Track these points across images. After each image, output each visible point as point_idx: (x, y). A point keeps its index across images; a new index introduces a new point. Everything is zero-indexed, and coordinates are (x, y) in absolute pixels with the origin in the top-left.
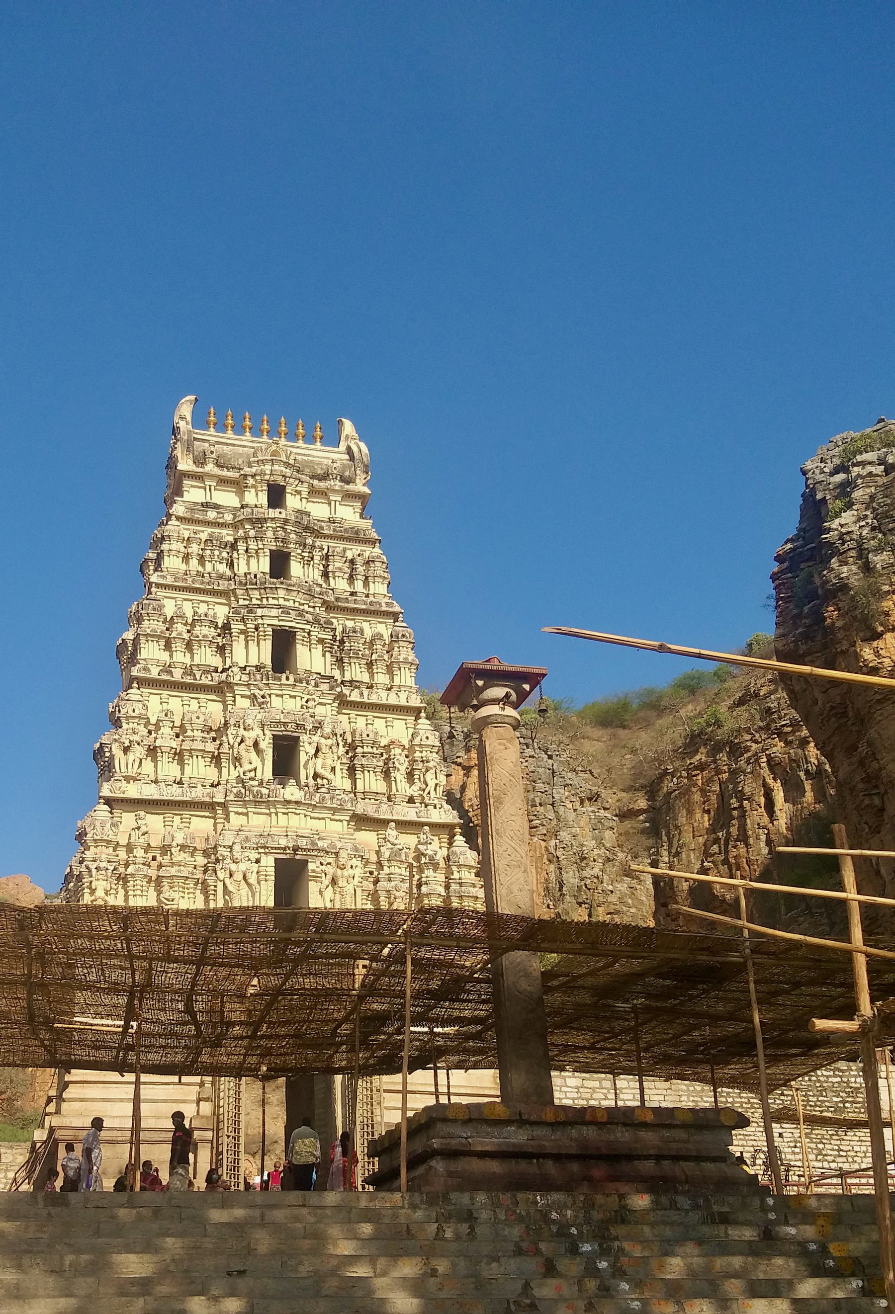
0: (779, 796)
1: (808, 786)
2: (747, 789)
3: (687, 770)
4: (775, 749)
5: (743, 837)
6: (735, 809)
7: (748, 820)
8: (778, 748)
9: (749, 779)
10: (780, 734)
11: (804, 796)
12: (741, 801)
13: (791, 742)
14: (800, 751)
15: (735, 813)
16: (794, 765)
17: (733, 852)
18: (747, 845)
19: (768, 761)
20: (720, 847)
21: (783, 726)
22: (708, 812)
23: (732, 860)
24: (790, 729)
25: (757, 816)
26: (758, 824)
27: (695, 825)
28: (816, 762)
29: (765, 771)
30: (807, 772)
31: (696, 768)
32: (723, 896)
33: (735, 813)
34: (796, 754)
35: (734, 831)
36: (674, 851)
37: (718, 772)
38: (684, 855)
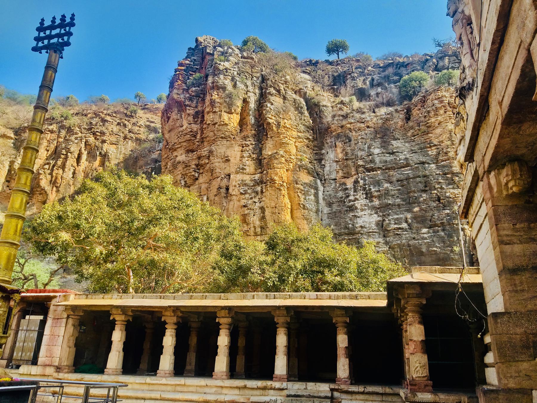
0: (84, 157)
1: (99, 158)
2: (72, 149)
4: (90, 139)
5: (63, 167)
6: (63, 154)
7: (68, 161)
8: (91, 139)
9: (75, 145)
10: (94, 134)
11: (95, 161)
12: (67, 152)
13: (98, 139)
14: (100, 144)
15: (63, 156)
17: (55, 171)
18: (63, 170)
19: (85, 142)
22: (48, 151)
23: (54, 174)
24: (99, 134)
25: (71, 161)
29: (83, 145)
30: (100, 153)
31: (49, 131)
33: (63, 156)
34: (99, 144)
35: (59, 163)
37: (59, 137)
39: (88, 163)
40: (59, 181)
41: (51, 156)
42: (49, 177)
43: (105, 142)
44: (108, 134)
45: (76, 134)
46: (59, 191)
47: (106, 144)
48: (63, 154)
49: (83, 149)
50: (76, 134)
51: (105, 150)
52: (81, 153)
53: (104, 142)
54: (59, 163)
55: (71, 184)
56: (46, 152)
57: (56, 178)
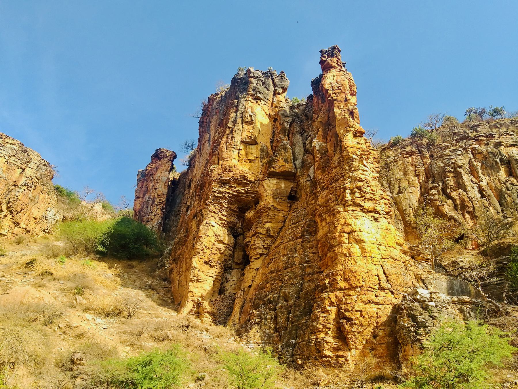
3: (401, 153)
5: (460, 185)
6: (450, 172)
7: (464, 178)
11: (498, 172)
14: (495, 150)
16: (491, 155)
17: (454, 195)
18: (465, 190)
20: (439, 192)
21: (480, 136)
22: (418, 176)
25: (467, 178)
26: (472, 181)
27: (410, 180)
28: (507, 156)
30: (501, 160)
32: (452, 216)
35: (451, 181)
36: (396, 191)
38: (406, 194)
39: (487, 177)
40: (469, 204)
41: (426, 181)
42: (449, 201)
43: (501, 145)
44: (497, 136)
45: (447, 147)
46: (476, 217)
47: (503, 147)
48: (450, 172)
49: (473, 160)
50: (447, 147)
51: (505, 154)
52: (473, 165)
53: (498, 145)
54: (451, 181)
55: (488, 205)
56: (417, 178)
57: (463, 201)
